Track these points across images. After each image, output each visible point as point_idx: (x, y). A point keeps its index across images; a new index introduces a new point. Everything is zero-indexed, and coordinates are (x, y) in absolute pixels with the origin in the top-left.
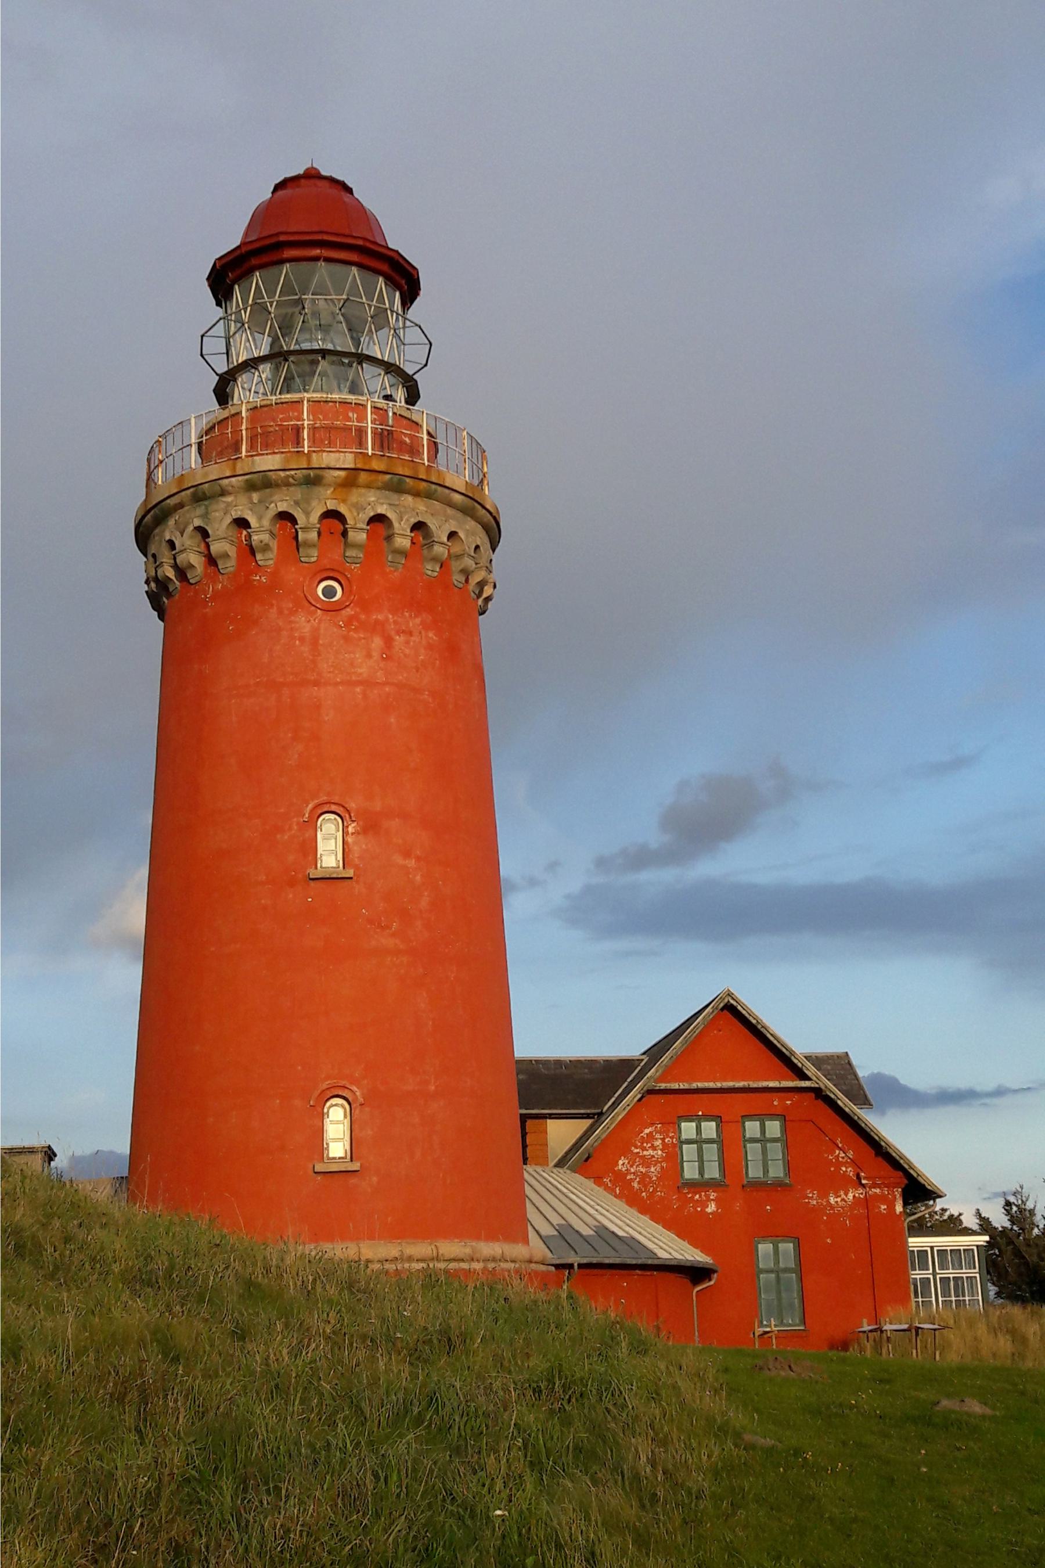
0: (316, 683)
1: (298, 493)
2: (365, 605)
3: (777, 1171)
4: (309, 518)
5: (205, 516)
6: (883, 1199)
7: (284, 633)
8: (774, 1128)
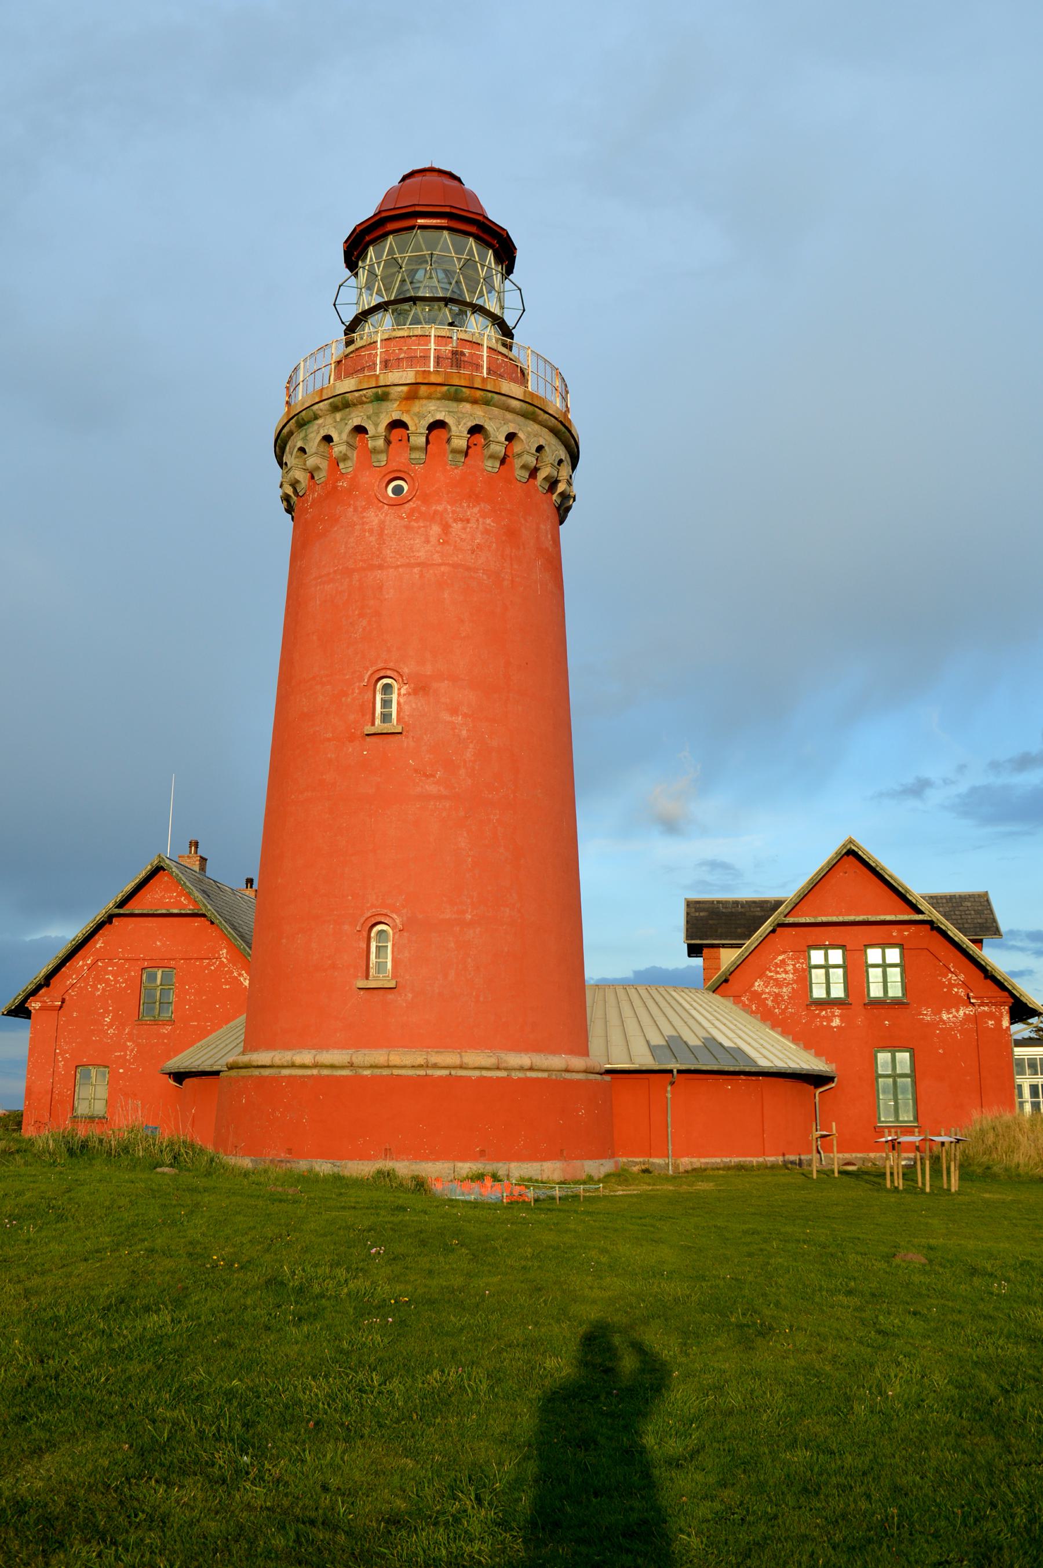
0: (380, 567)
1: (370, 408)
2: (426, 499)
3: (895, 991)
4: (377, 428)
5: (305, 439)
6: (991, 1015)
7: (357, 527)
8: (893, 955)
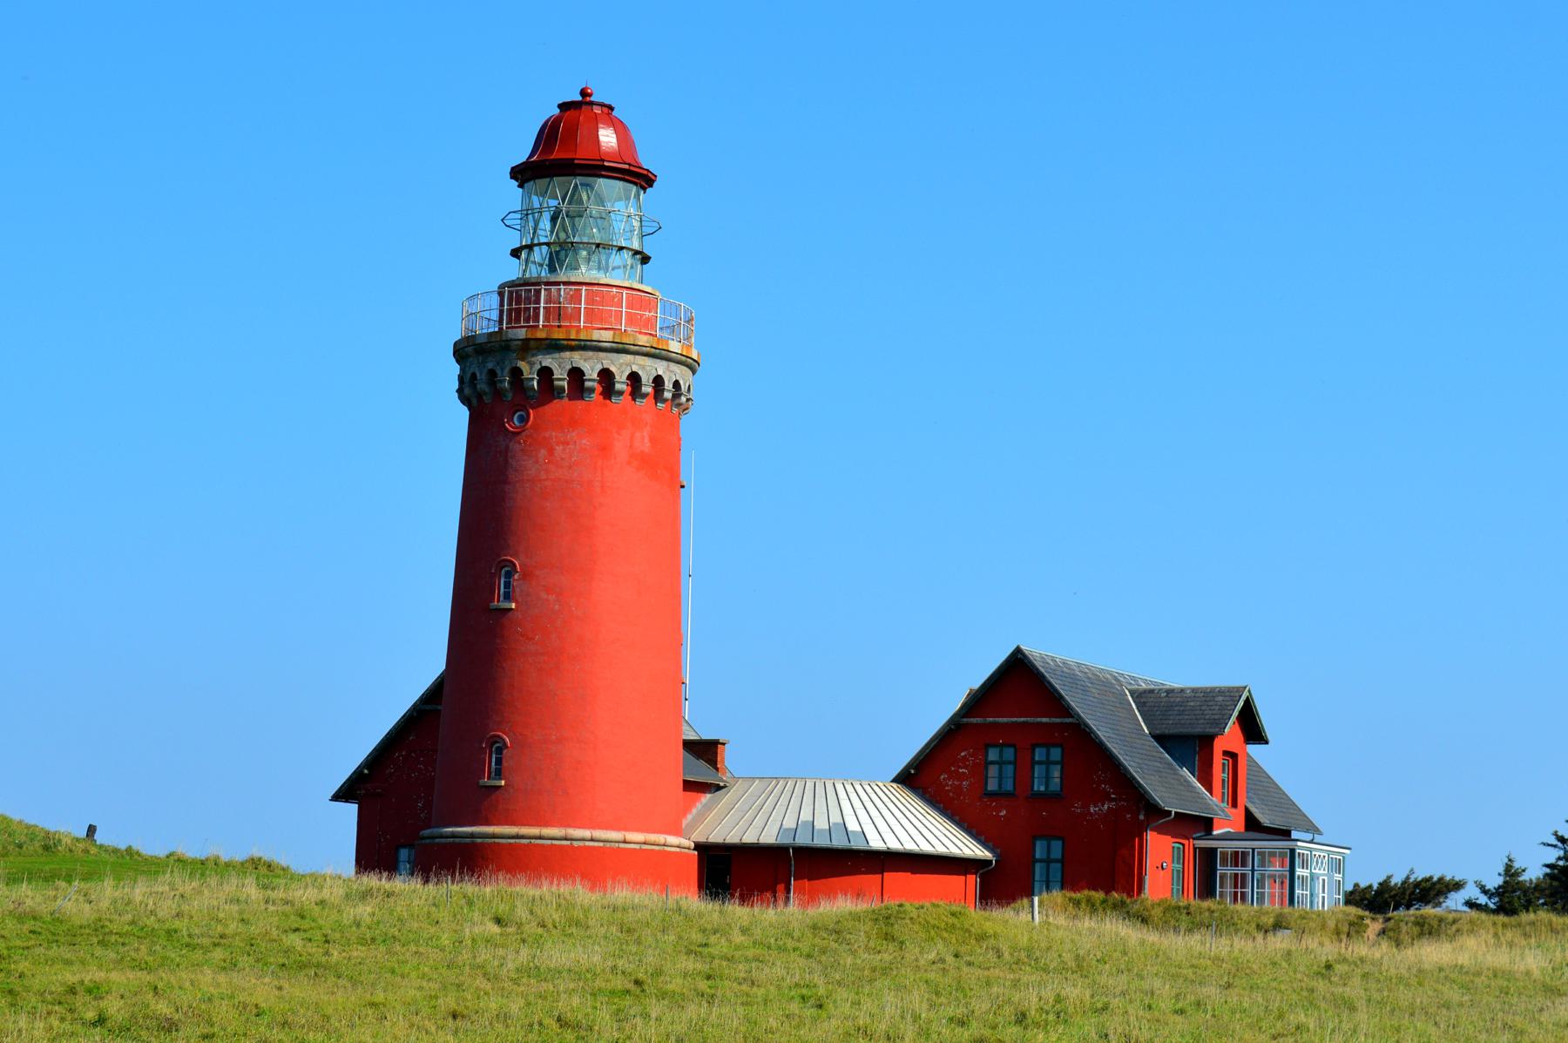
8: (1056, 754)
